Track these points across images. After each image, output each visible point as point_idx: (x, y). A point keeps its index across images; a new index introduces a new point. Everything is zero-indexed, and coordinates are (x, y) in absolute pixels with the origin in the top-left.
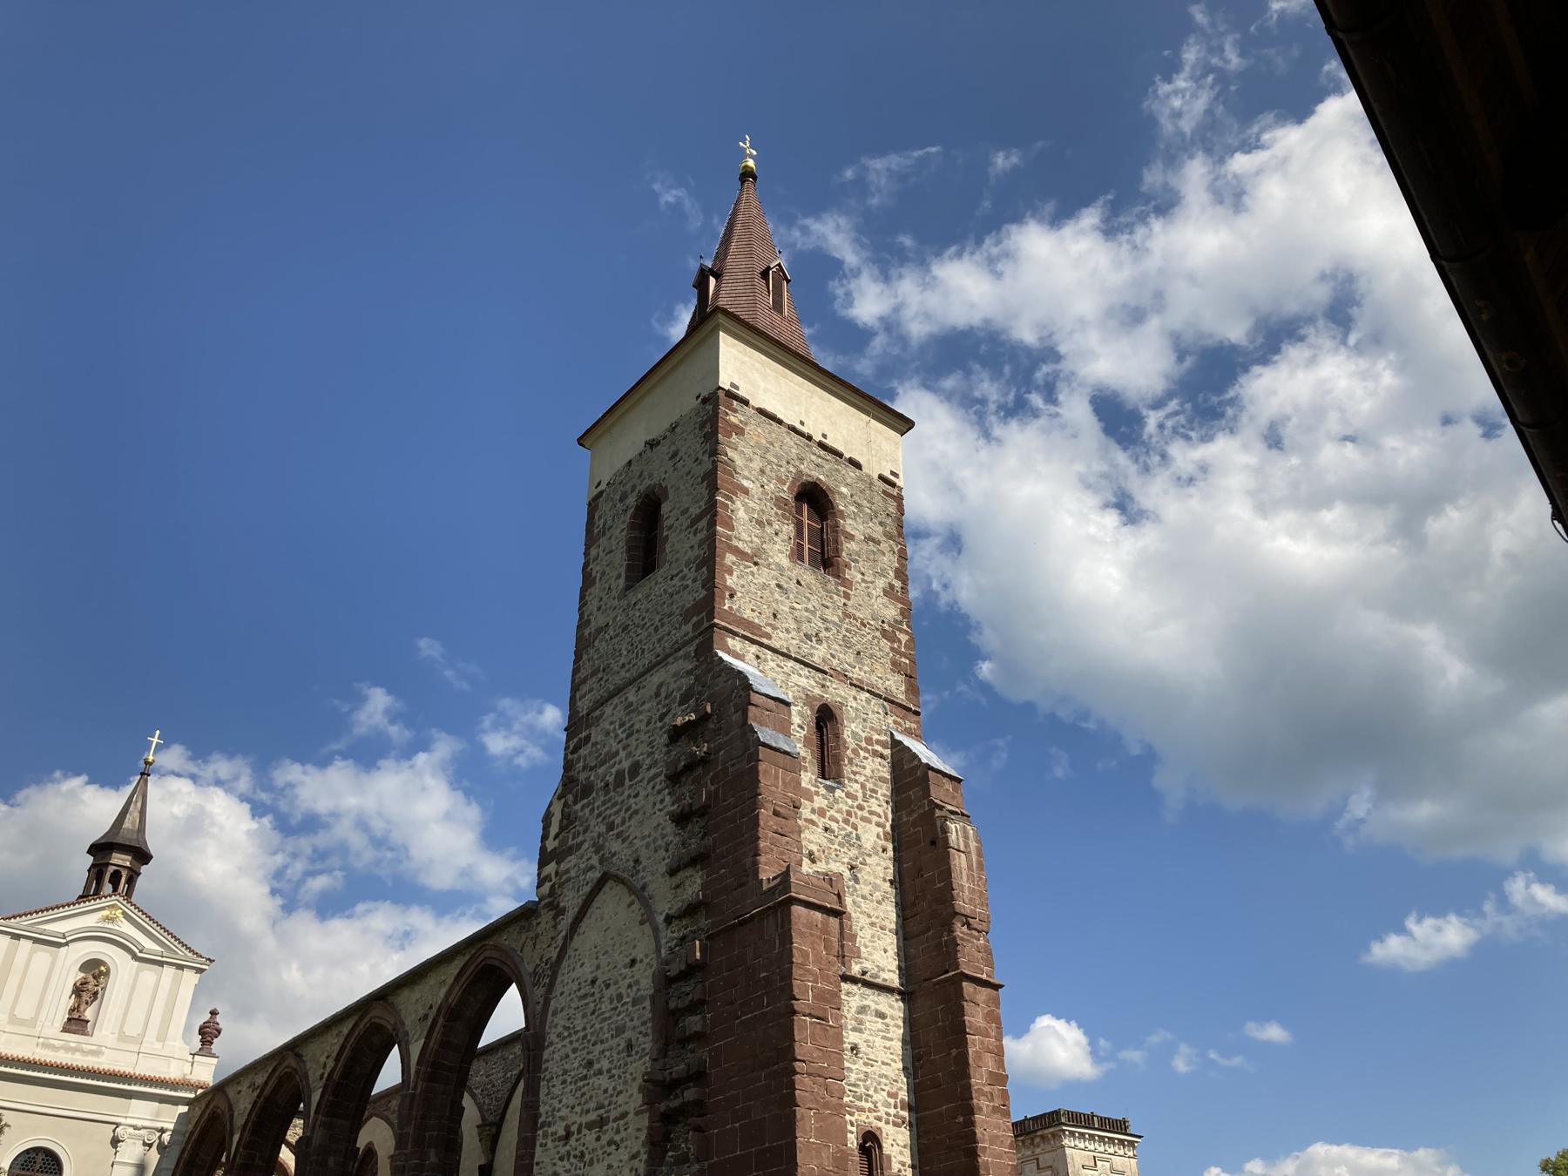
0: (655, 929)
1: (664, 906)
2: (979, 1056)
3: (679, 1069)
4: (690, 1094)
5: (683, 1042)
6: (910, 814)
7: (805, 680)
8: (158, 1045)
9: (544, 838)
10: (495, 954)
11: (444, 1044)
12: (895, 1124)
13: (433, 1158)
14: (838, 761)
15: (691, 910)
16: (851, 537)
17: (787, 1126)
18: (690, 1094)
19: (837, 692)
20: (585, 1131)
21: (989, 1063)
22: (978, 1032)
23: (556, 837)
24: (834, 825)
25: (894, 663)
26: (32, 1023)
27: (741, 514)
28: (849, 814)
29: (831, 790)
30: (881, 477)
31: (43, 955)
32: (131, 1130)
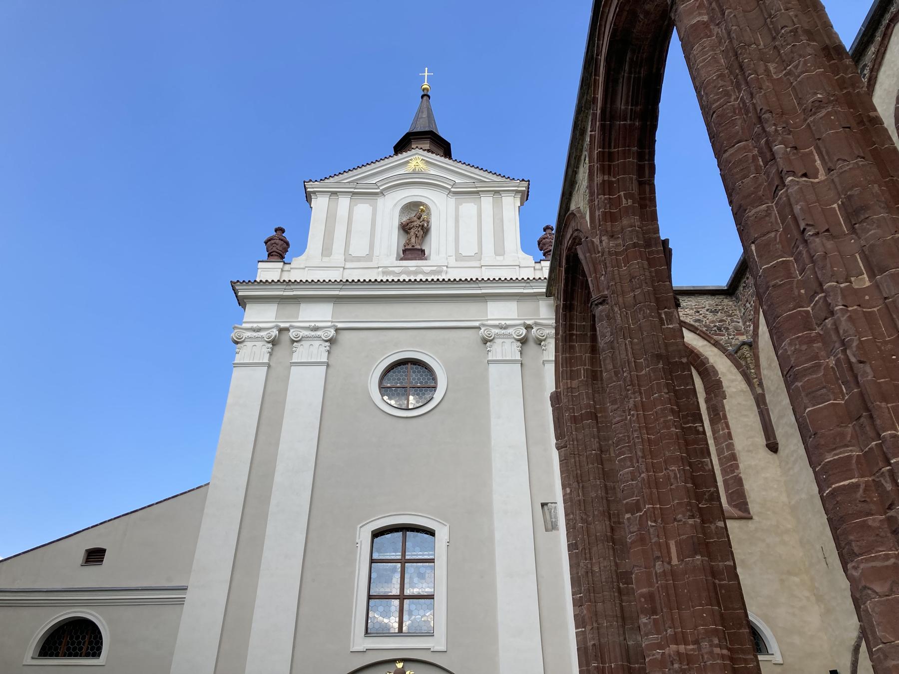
8: (500, 258)
26: (369, 257)
31: (363, 209)
32: (497, 331)
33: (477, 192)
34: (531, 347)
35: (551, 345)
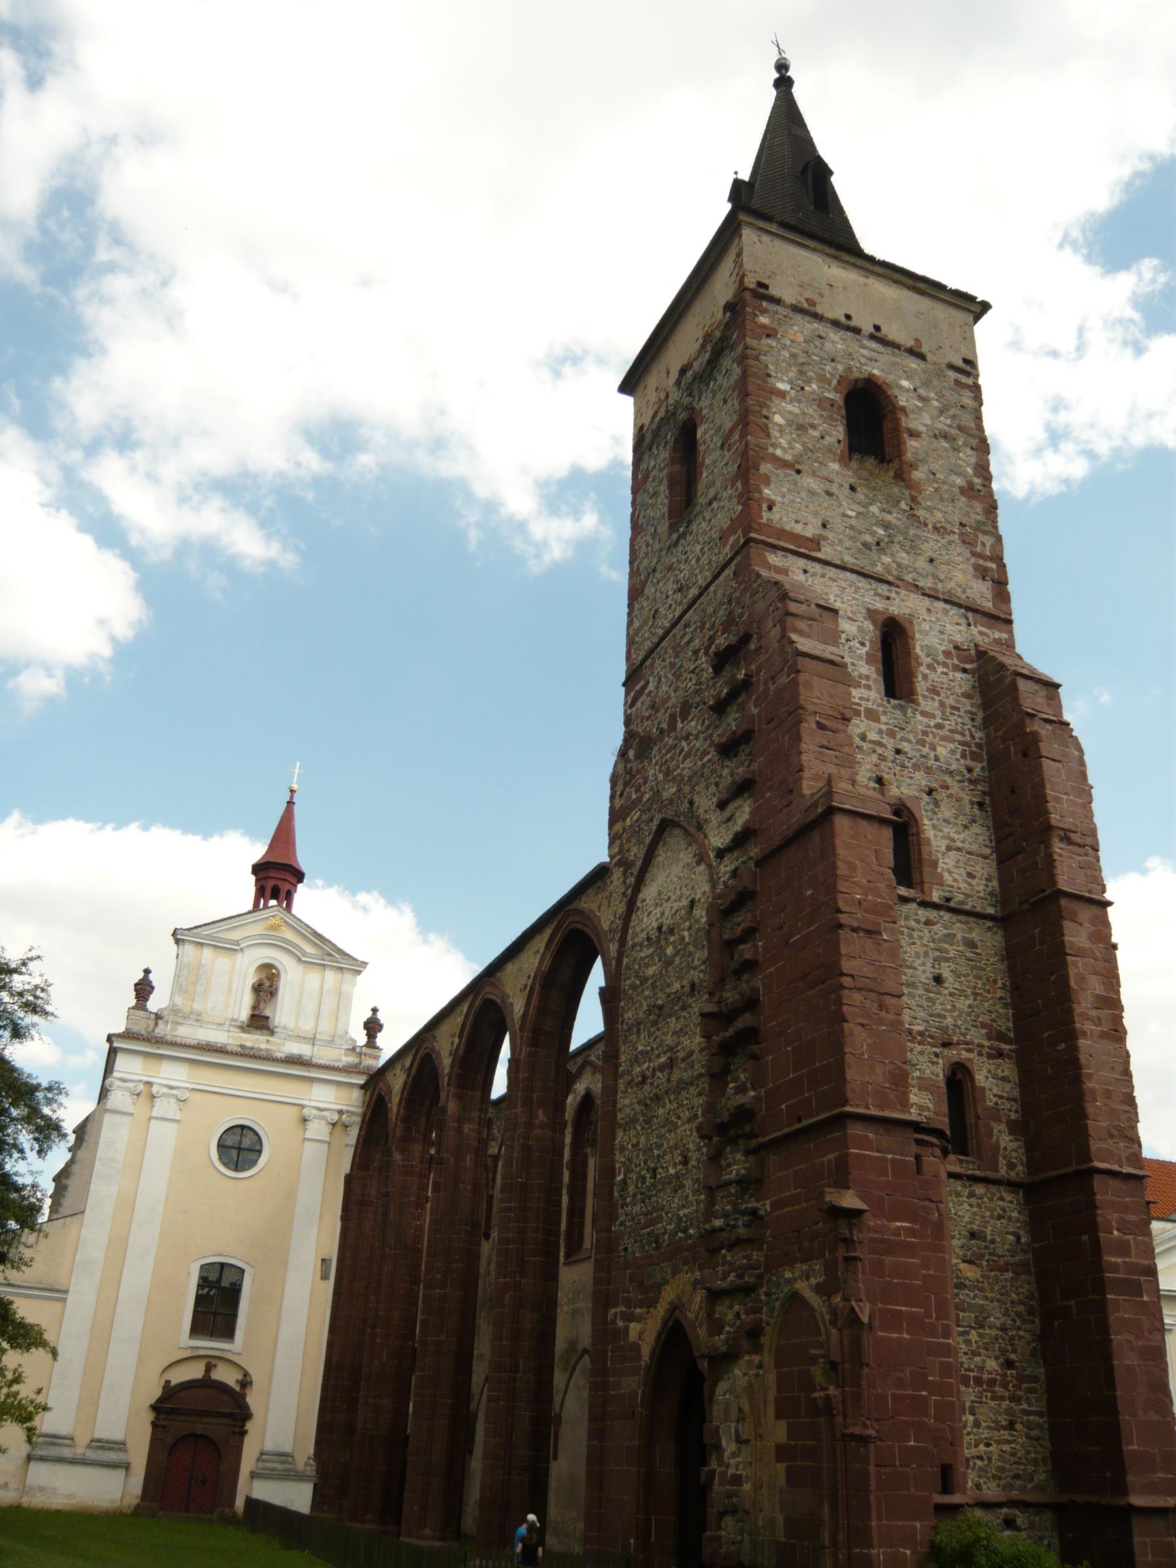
0: (710, 866)
1: (718, 838)
2: (1082, 979)
3: (731, 996)
4: (741, 1023)
5: (738, 974)
6: (996, 730)
7: (868, 596)
9: (612, 797)
10: (577, 918)
11: (542, 1011)
12: (990, 1056)
13: (541, 1116)
14: (910, 676)
15: (741, 840)
16: (914, 434)
17: (836, 1044)
18: (741, 1023)
19: (903, 604)
20: (659, 1074)
21: (1095, 986)
22: (1081, 953)
23: (621, 796)
24: (905, 746)
25: (977, 567)
27: (778, 419)
28: (925, 733)
29: (902, 709)
30: (951, 367)
32: (314, 1112)
33: (324, 965)
34: (338, 1129)
35: (354, 1132)
